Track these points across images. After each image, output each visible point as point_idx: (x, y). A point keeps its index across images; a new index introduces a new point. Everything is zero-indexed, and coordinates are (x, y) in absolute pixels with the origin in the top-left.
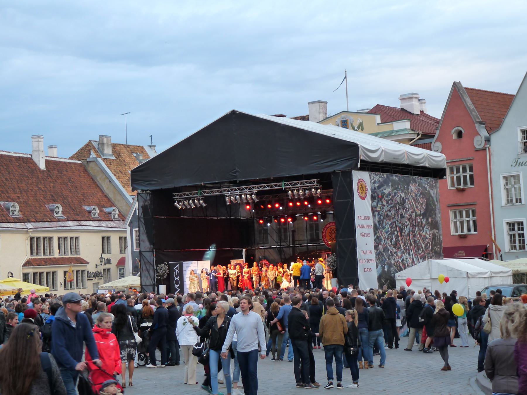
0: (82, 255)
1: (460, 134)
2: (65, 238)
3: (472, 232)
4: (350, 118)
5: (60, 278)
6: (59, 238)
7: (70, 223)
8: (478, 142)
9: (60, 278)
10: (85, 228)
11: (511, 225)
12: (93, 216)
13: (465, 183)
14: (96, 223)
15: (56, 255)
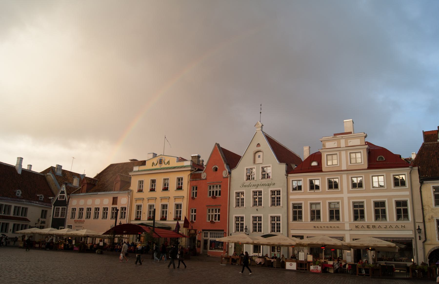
0: (28, 217)
1: (216, 169)
2: (19, 207)
3: (217, 221)
4: (164, 158)
5: (11, 226)
6: (15, 207)
7: (24, 200)
8: (225, 174)
9: (11, 226)
10: (33, 204)
11: (237, 218)
12: (40, 199)
13: (216, 194)
14: (40, 203)
15: (12, 215)
